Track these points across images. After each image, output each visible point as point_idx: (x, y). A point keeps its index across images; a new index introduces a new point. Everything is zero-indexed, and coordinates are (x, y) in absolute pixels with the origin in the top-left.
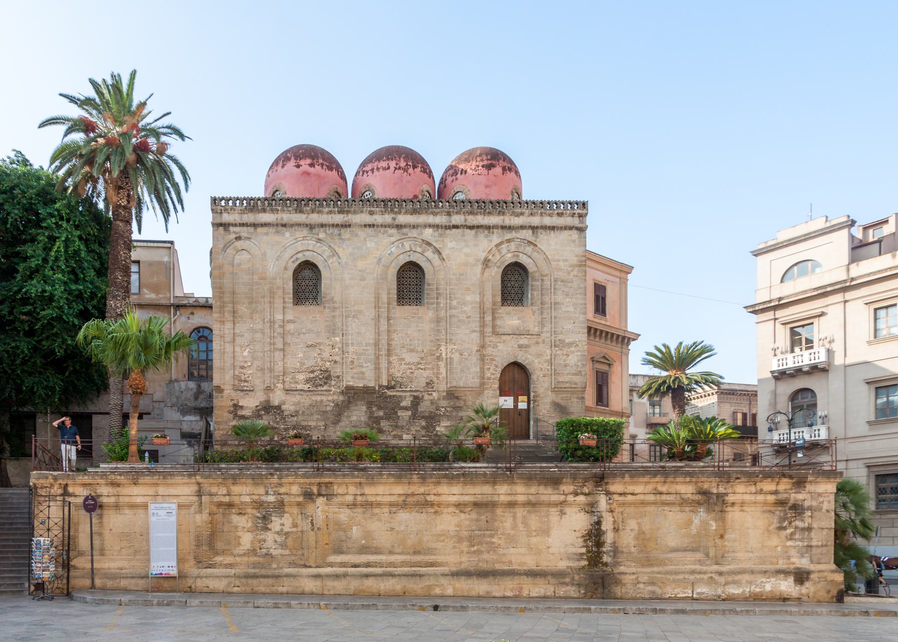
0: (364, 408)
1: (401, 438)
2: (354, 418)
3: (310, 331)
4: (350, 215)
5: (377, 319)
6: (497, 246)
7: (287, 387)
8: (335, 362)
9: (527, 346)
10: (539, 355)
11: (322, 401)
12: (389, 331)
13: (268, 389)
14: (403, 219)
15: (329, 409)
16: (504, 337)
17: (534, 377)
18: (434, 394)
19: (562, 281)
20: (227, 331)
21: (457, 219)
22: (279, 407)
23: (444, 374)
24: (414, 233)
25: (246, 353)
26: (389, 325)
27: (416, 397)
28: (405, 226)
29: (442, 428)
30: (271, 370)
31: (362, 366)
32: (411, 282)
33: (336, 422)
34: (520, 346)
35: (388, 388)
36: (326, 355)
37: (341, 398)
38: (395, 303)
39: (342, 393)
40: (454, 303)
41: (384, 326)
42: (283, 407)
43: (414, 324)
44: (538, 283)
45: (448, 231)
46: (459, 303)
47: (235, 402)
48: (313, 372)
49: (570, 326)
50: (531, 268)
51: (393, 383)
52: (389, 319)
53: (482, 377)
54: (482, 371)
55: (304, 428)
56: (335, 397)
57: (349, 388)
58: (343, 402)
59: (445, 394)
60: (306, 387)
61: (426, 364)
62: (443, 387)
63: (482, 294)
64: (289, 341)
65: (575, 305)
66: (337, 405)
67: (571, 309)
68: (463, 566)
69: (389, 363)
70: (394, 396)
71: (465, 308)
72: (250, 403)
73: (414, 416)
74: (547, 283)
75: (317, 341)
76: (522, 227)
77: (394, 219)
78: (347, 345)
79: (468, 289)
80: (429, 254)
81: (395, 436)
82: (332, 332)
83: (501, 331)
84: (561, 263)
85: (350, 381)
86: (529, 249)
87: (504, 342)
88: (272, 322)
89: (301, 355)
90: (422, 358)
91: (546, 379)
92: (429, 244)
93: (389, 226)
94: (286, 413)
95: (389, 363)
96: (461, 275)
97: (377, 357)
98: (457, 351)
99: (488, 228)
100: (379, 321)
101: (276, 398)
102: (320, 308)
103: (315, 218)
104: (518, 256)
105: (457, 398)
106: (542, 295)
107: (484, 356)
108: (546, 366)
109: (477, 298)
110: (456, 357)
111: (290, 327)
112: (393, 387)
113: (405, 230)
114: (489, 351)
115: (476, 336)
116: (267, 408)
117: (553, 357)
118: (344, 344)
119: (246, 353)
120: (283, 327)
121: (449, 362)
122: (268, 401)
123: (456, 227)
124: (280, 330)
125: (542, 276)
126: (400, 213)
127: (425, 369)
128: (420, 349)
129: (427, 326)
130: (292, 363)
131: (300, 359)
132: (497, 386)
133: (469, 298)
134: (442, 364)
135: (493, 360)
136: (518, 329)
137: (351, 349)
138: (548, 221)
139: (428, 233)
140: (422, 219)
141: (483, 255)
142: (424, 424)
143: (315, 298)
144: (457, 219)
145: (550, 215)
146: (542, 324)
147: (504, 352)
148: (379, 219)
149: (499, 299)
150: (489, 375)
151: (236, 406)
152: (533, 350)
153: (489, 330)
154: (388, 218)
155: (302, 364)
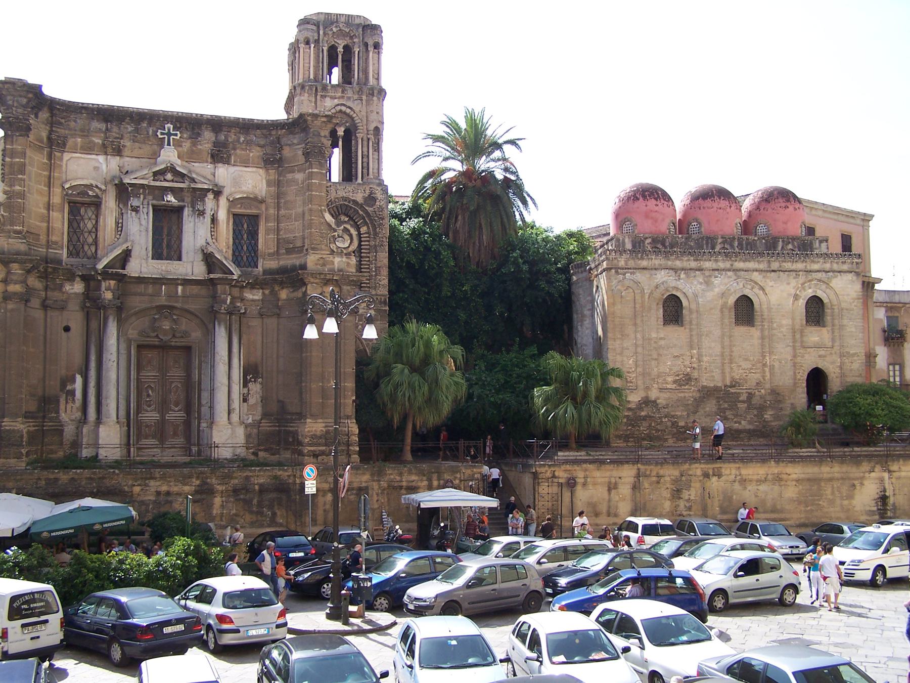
0: (714, 402)
1: (740, 423)
2: (708, 409)
3: (675, 346)
6: (802, 284)
9: (825, 356)
10: (833, 363)
13: (647, 388)
15: (690, 402)
16: (809, 350)
17: (830, 378)
18: (763, 391)
21: (775, 265)
22: (655, 402)
25: (631, 362)
26: (730, 341)
27: (749, 393)
28: (740, 270)
29: (768, 416)
30: (649, 374)
32: (745, 310)
33: (695, 412)
34: (820, 356)
35: (732, 386)
36: (687, 363)
39: (699, 390)
40: (775, 325)
42: (658, 401)
43: (747, 340)
45: (768, 274)
48: (678, 375)
49: (853, 342)
50: (826, 301)
52: (730, 337)
53: (795, 379)
54: (795, 373)
55: (673, 416)
57: (703, 387)
60: (673, 386)
62: (768, 386)
63: (793, 319)
65: (856, 326)
67: (853, 330)
68: (802, 520)
72: (634, 398)
73: (749, 408)
74: (836, 310)
78: (702, 356)
79: (783, 316)
80: (756, 290)
81: (736, 423)
82: (691, 347)
83: (806, 345)
85: (705, 382)
86: (824, 287)
92: (756, 283)
93: (729, 270)
95: (732, 368)
97: (723, 364)
101: (653, 394)
103: (678, 264)
108: (838, 370)
109: (790, 322)
110: (776, 364)
111: (662, 343)
112: (734, 386)
114: (799, 359)
115: (789, 349)
116: (646, 402)
117: (842, 364)
118: (700, 356)
119: (631, 362)
121: (772, 368)
122: (647, 397)
123: (773, 271)
124: (654, 345)
129: (756, 342)
132: (805, 385)
133: (784, 322)
134: (767, 369)
137: (705, 359)
138: (835, 267)
139: (756, 276)
140: (751, 265)
141: (793, 292)
144: (775, 265)
145: (837, 263)
146: (833, 340)
147: (810, 361)
148: (721, 265)
152: (828, 359)
153: (798, 344)
154: (727, 265)
155: (671, 370)
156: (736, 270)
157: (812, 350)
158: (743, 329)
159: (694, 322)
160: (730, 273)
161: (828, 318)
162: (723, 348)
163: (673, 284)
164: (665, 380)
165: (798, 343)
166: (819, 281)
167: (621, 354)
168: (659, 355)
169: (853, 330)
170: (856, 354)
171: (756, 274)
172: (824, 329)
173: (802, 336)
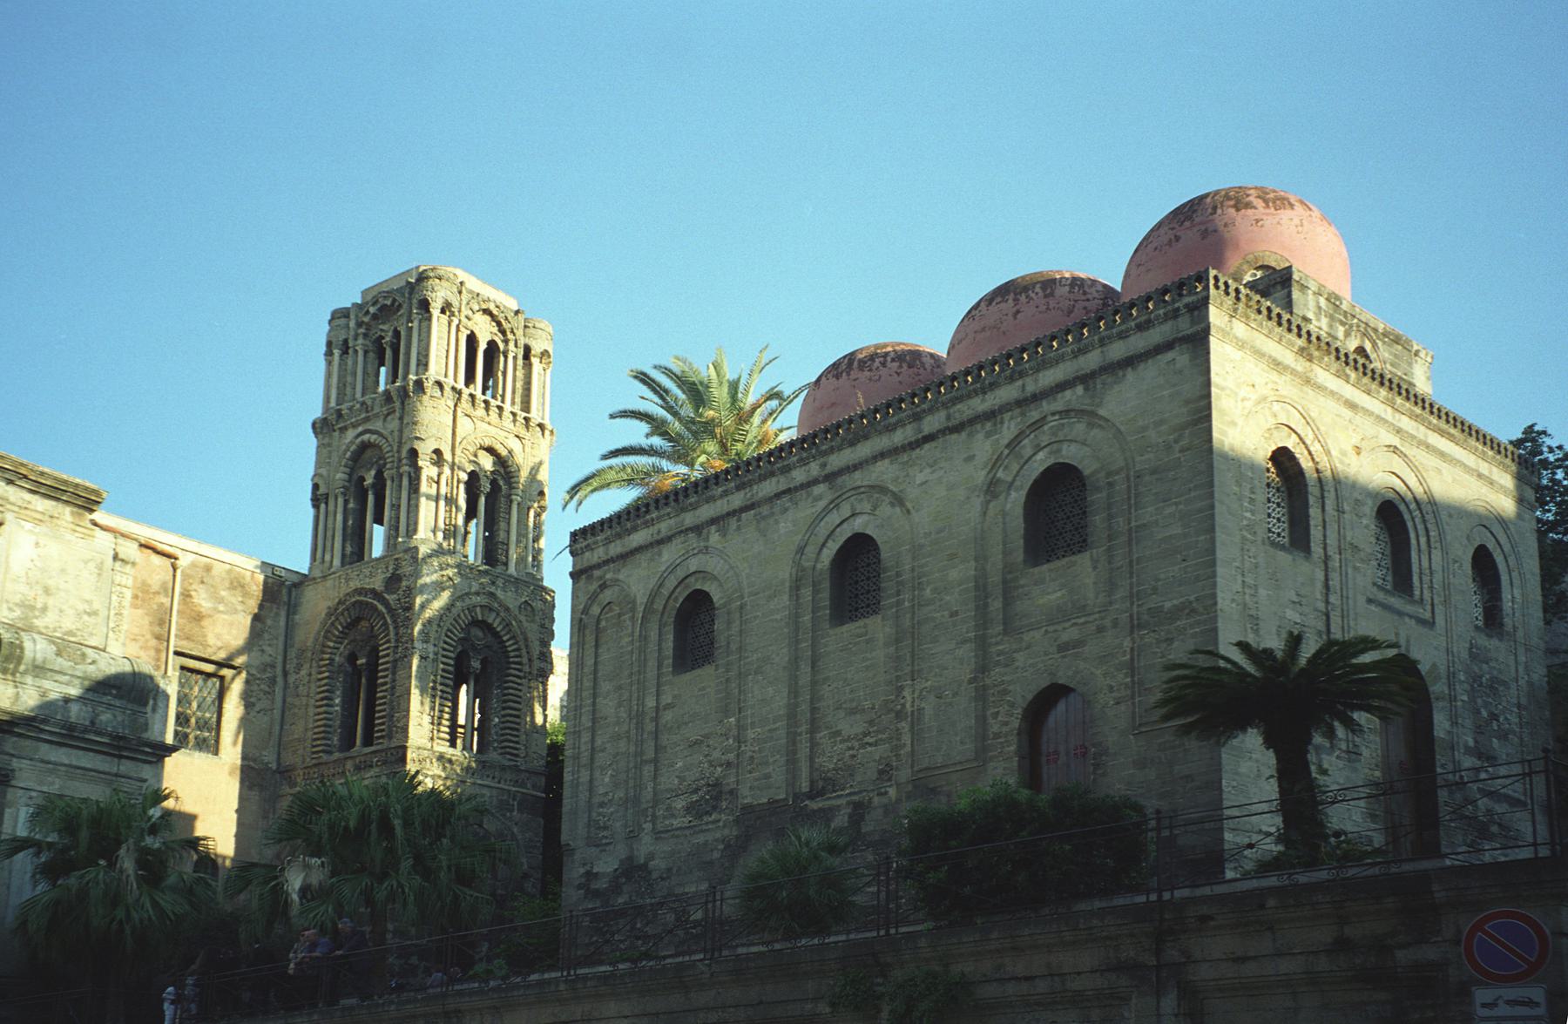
5: (795, 661)
7: (659, 827)
8: (729, 764)
9: (1079, 643)
11: (706, 843)
12: (814, 683)
13: (632, 836)
14: (837, 461)
18: (892, 792)
20: (583, 748)
22: (645, 865)
23: (908, 749)
24: (858, 478)
27: (858, 806)
31: (767, 763)
32: (856, 576)
34: (1063, 648)
39: (737, 821)
43: (860, 655)
46: (934, 590)
47: (588, 868)
48: (696, 791)
51: (821, 783)
54: (982, 720)
56: (726, 832)
57: (748, 809)
58: (737, 837)
59: (910, 788)
61: (878, 732)
63: (981, 558)
64: (665, 742)
66: (728, 846)
69: (814, 745)
72: (607, 865)
77: (824, 465)
79: (952, 557)
80: (886, 510)
82: (726, 712)
85: (747, 797)
88: (640, 715)
90: (871, 723)
91: (1123, 707)
92: (883, 490)
94: (655, 875)
95: (814, 745)
96: (940, 531)
97: (793, 738)
100: (797, 668)
105: (934, 791)
107: (985, 688)
110: (929, 706)
113: (839, 480)
115: (967, 652)
116: (632, 870)
118: (741, 727)
120: (656, 719)
126: (832, 450)
127: (875, 744)
128: (867, 704)
130: (668, 781)
131: (682, 768)
135: (1006, 692)
137: (751, 734)
139: (884, 471)
141: (981, 476)
142: (870, 858)
144: (932, 423)
149: (1019, 556)
150: (995, 728)
151: (590, 876)
155: (682, 779)
157: (1037, 635)
159: (733, 647)
160: (820, 489)
162: (794, 692)
163: (693, 564)
164: (669, 808)
167: (592, 759)
168: (657, 749)
170: (1179, 609)
172: (1083, 561)
173: (1008, 600)
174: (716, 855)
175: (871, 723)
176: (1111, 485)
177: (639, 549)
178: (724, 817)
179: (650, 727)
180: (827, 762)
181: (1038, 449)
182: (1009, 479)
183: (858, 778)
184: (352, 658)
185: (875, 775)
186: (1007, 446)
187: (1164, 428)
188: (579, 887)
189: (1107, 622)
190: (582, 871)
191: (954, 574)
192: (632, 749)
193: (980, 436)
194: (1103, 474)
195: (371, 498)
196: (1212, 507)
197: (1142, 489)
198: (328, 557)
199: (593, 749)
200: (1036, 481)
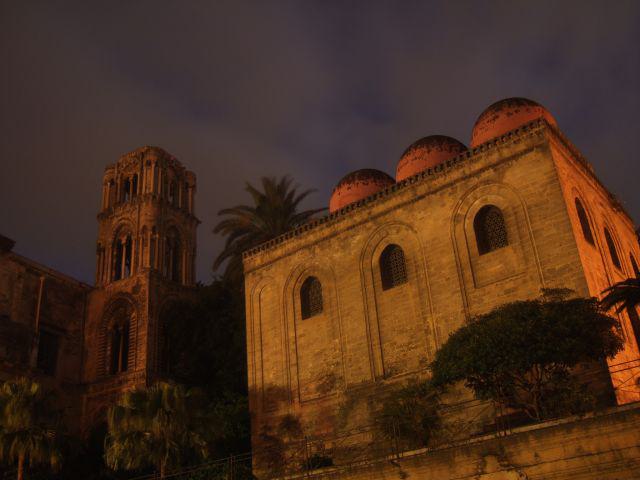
2: (358, 417)
4: (336, 226)
5: (366, 311)
6: (463, 198)
8: (338, 363)
19: (536, 206)
21: (422, 189)
25: (271, 376)
32: (392, 267)
34: (507, 292)
35: (385, 376)
37: (345, 400)
38: (381, 289)
39: (346, 393)
40: (432, 269)
41: (373, 317)
43: (401, 302)
44: (513, 218)
45: (416, 204)
46: (435, 269)
56: (341, 399)
57: (351, 386)
58: (347, 402)
63: (457, 251)
67: (554, 231)
70: (392, 384)
71: (443, 272)
75: (323, 348)
76: (482, 170)
84: (531, 188)
85: (350, 379)
87: (489, 293)
89: (311, 365)
92: (401, 223)
96: (433, 240)
97: (371, 347)
98: (443, 317)
99: (451, 184)
102: (322, 315)
104: (486, 200)
106: (518, 228)
110: (442, 326)
112: (390, 375)
115: (458, 297)
123: (422, 197)
125: (514, 208)
126: (373, 206)
127: (416, 347)
133: (444, 260)
136: (501, 273)
137: (348, 347)
138: (506, 153)
141: (450, 213)
143: (322, 309)
146: (526, 260)
148: (357, 218)
154: (365, 214)
155: (313, 373)
156: (374, 218)
157: (493, 287)
158: (392, 291)
159: (333, 303)
160: (370, 224)
161: (512, 230)
162: (368, 324)
165: (468, 278)
166: (487, 182)
169: (554, 231)
171: (399, 211)
174: (336, 412)
175: (412, 337)
176: (516, 213)
177: (279, 258)
178: (338, 391)
179: (293, 347)
180: (392, 355)
181: (476, 199)
182: (464, 214)
183: (409, 366)
184: (116, 327)
185: (418, 364)
186: (461, 198)
187: (537, 186)
188: (261, 435)
189: (528, 277)
190: (261, 426)
191: (444, 260)
192: (284, 359)
193: (447, 195)
194: (510, 208)
195: (124, 249)
196: (569, 219)
197: (533, 214)
198: (105, 278)
199: (262, 361)
200: (477, 214)
